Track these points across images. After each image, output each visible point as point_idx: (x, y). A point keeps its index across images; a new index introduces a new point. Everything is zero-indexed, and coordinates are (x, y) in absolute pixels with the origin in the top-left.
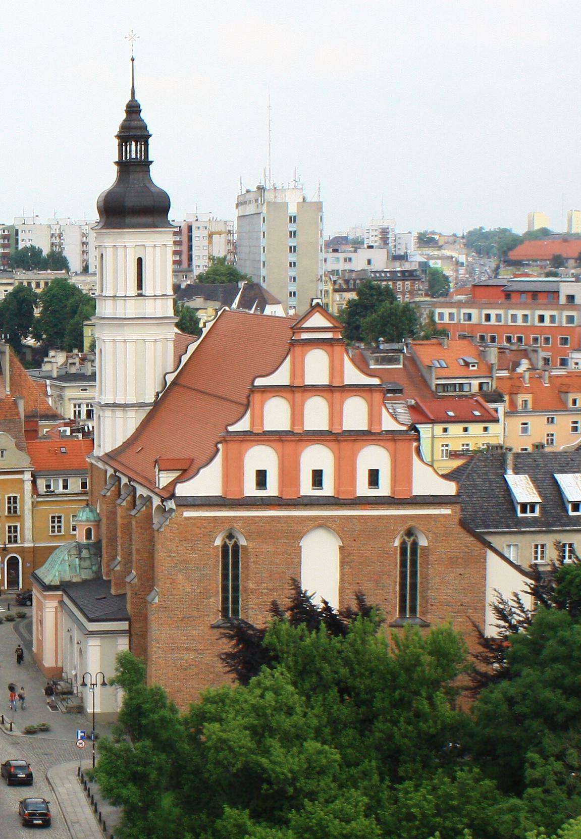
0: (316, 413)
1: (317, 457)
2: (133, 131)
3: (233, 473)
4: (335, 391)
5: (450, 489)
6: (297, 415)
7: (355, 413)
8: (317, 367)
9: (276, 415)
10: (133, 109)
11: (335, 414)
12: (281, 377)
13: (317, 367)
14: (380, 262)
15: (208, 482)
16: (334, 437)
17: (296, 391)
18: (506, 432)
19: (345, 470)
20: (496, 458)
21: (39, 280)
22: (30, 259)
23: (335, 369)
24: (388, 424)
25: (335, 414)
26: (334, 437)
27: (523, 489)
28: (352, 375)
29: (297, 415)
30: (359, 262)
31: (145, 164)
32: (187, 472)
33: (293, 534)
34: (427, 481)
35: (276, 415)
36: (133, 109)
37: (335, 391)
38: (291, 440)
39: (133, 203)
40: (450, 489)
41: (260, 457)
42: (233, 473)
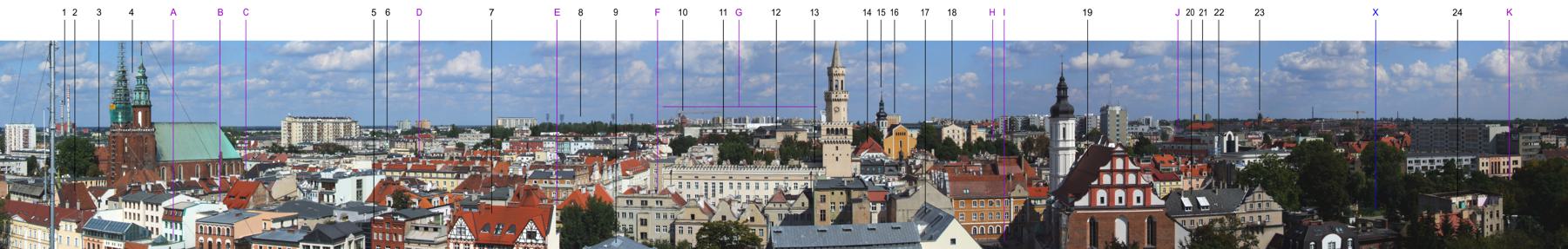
0: (1119, 179)
1: (1119, 193)
2: (1062, 87)
3: (1092, 199)
4: (1125, 171)
5: (1162, 203)
6: (1113, 179)
7: (1132, 179)
8: (1119, 164)
9: (1106, 179)
10: (1062, 79)
11: (1125, 179)
12: (1108, 167)
13: (1119, 164)
14: (1146, 128)
15: (1084, 201)
16: (1125, 187)
17: (1112, 172)
18: (1184, 184)
19: (1129, 197)
20: (1179, 193)
21: (1034, 135)
22: (1034, 128)
23: (1125, 164)
24: (1143, 182)
25: (1125, 179)
26: (1125, 187)
27: (1187, 202)
28: (1131, 166)
29: (1113, 179)
30: (1140, 129)
31: (1065, 97)
32: (1079, 197)
33: (1112, 218)
34: (1155, 200)
35: (1106, 179)
36: (1062, 79)
37: (1125, 171)
38: (1110, 188)
39: (1060, 111)
40: (1162, 203)
41: (1101, 193)
42: (1092, 199)
